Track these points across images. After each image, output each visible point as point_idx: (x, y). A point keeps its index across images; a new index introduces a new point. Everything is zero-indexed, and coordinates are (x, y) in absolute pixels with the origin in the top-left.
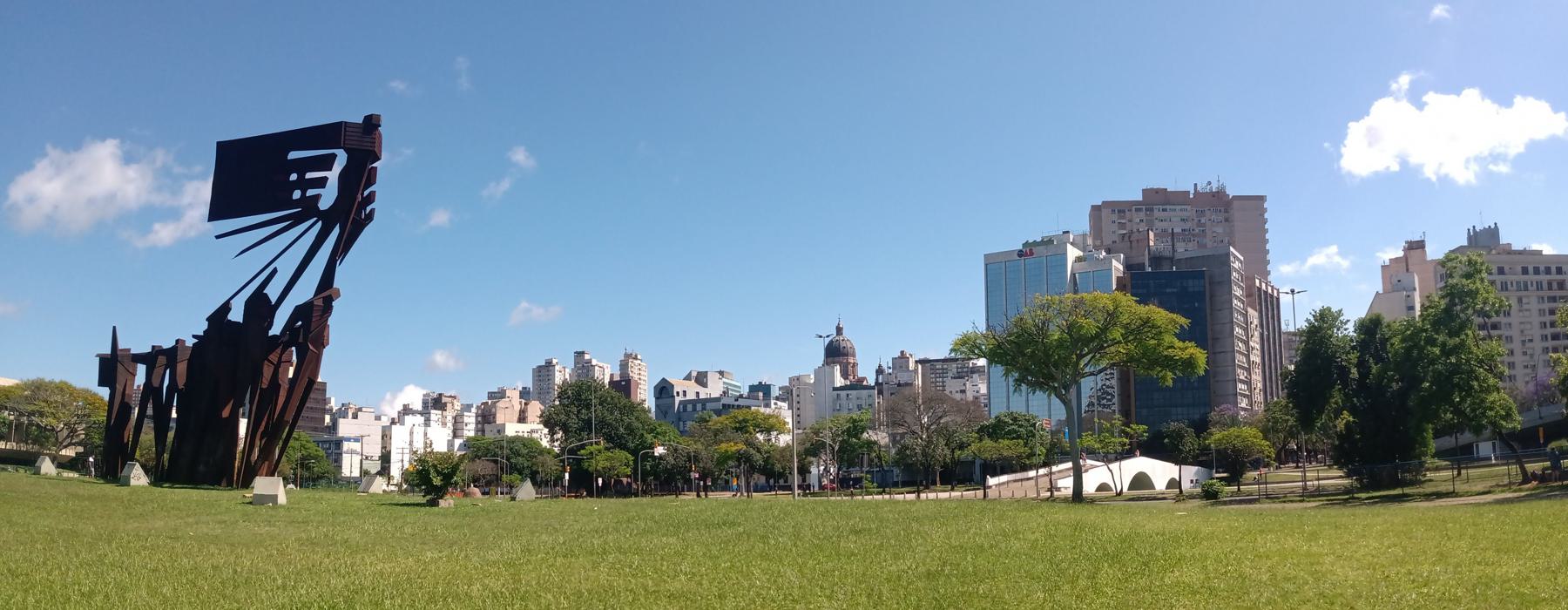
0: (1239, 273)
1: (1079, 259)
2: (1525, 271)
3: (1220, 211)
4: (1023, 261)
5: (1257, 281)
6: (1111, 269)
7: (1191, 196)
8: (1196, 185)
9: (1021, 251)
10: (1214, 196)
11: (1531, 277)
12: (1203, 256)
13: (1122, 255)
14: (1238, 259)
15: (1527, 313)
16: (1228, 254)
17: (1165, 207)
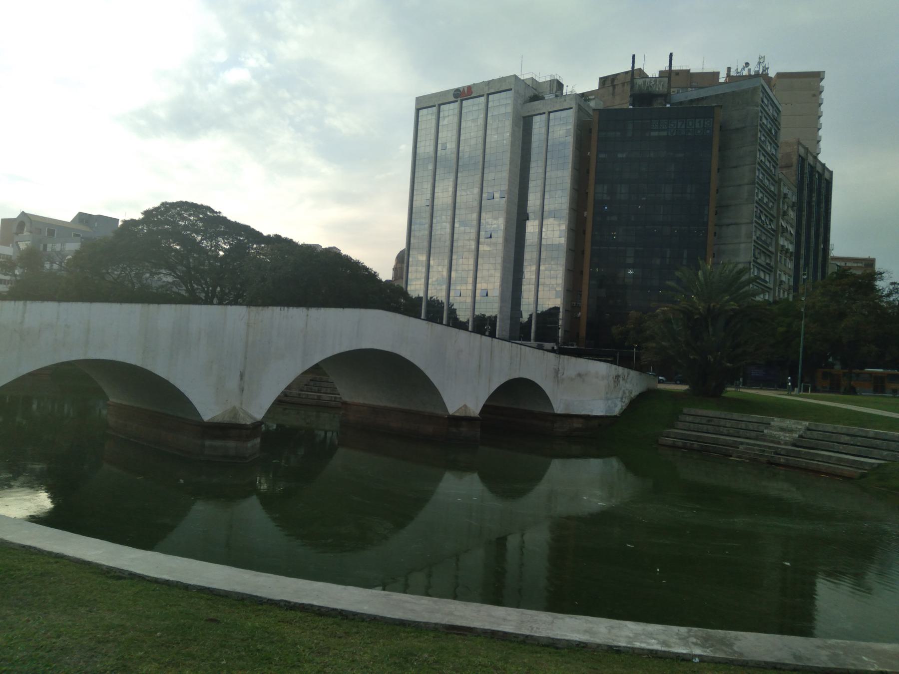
8: (729, 69)
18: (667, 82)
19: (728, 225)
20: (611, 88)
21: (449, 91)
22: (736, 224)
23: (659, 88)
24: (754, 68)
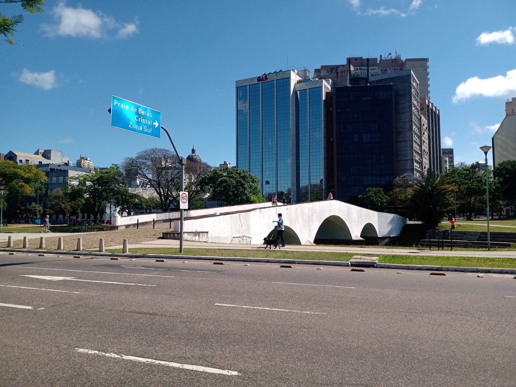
0: (416, 91)
1: (299, 82)
3: (397, 69)
4: (261, 84)
5: (427, 101)
6: (321, 87)
7: (378, 62)
8: (381, 56)
9: (259, 77)
10: (393, 62)
12: (390, 78)
13: (331, 80)
14: (416, 82)
16: (409, 75)
17: (361, 68)
18: (367, 73)
19: (401, 142)
20: (336, 75)
21: (254, 78)
22: (404, 141)
23: (363, 76)
24: (393, 56)
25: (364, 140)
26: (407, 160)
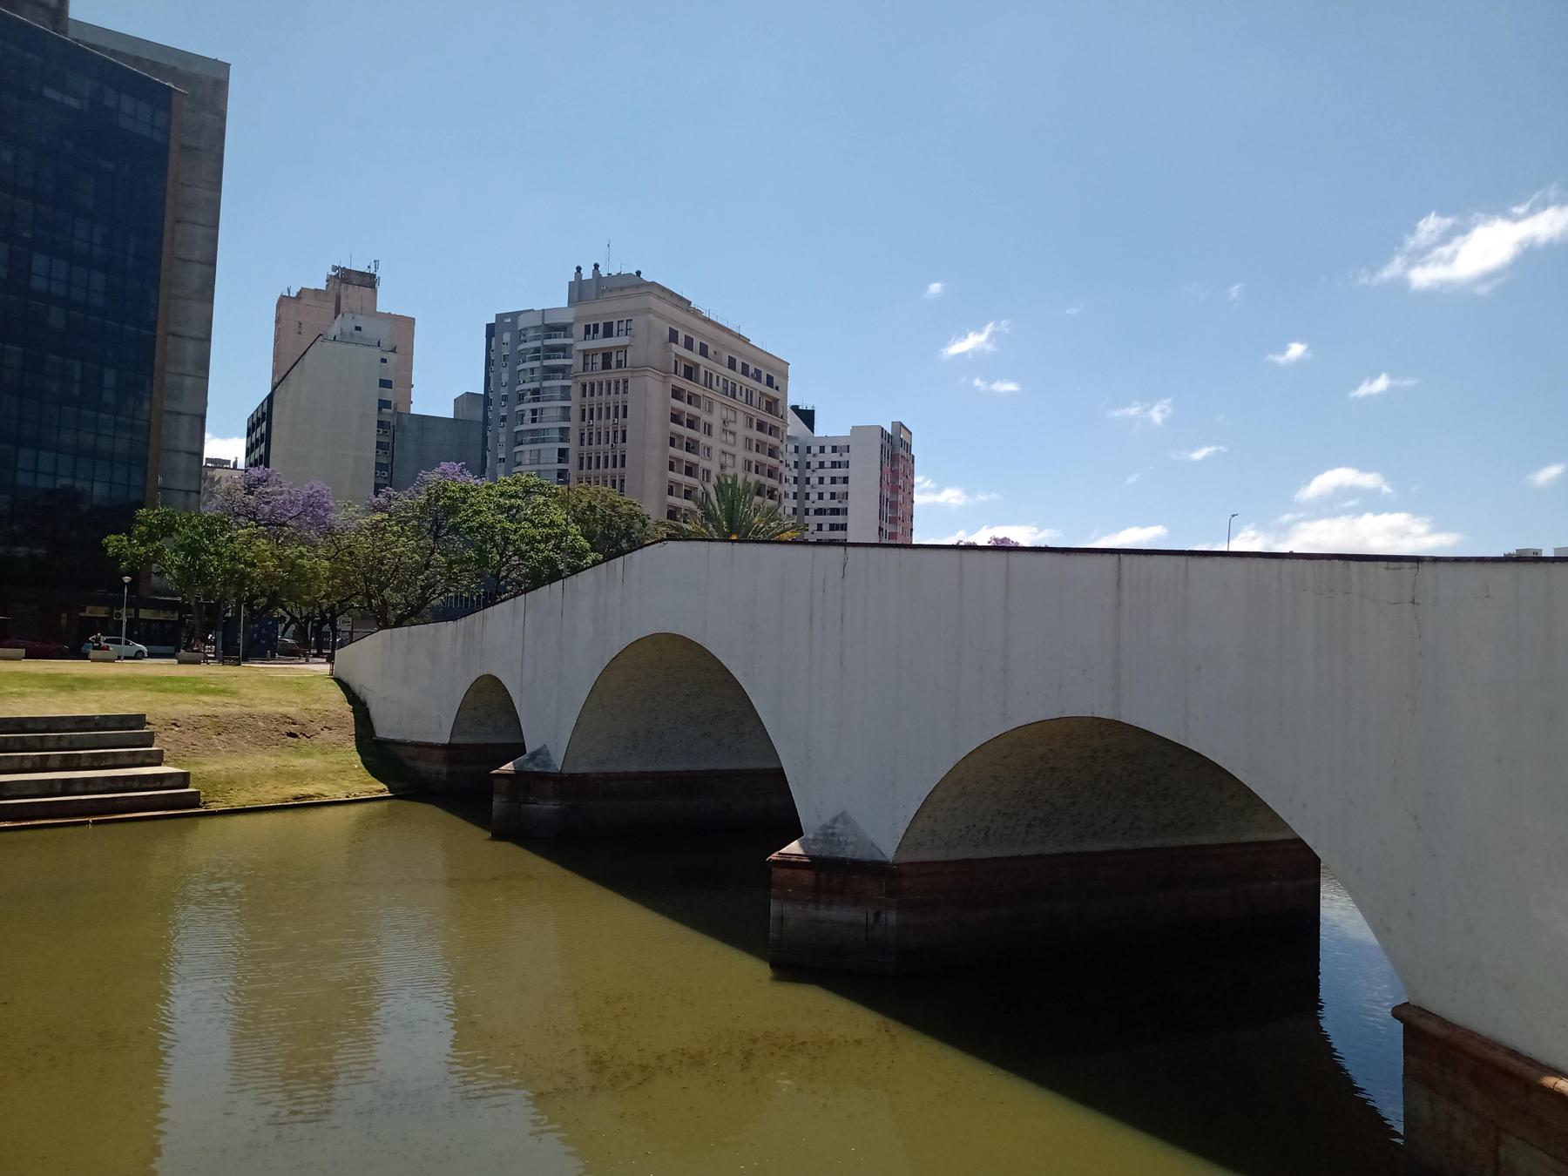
2: (732, 364)
11: (736, 376)
15: (730, 438)
25: (37, 283)
26: (178, 413)
